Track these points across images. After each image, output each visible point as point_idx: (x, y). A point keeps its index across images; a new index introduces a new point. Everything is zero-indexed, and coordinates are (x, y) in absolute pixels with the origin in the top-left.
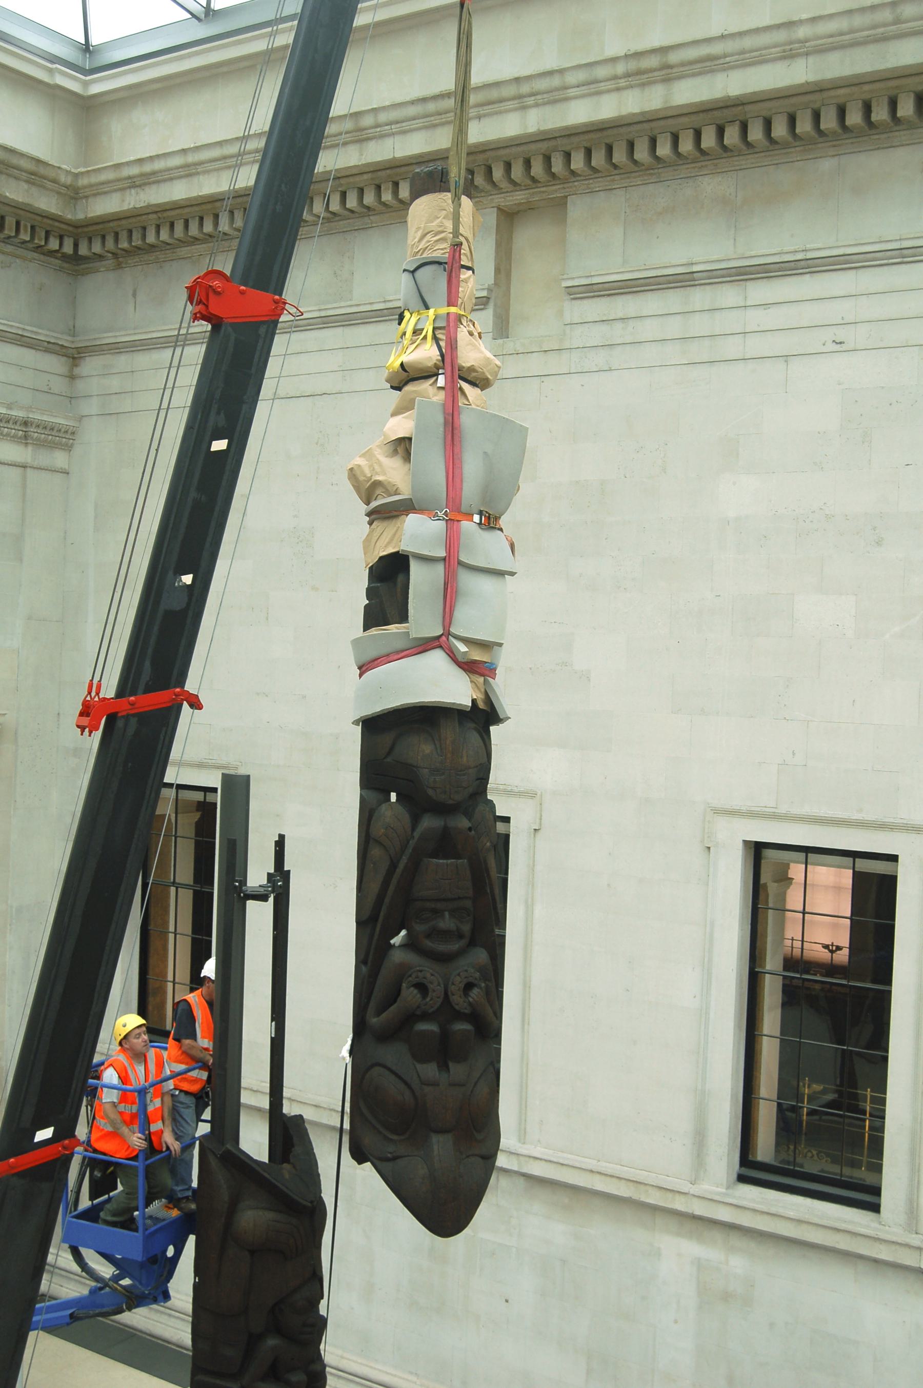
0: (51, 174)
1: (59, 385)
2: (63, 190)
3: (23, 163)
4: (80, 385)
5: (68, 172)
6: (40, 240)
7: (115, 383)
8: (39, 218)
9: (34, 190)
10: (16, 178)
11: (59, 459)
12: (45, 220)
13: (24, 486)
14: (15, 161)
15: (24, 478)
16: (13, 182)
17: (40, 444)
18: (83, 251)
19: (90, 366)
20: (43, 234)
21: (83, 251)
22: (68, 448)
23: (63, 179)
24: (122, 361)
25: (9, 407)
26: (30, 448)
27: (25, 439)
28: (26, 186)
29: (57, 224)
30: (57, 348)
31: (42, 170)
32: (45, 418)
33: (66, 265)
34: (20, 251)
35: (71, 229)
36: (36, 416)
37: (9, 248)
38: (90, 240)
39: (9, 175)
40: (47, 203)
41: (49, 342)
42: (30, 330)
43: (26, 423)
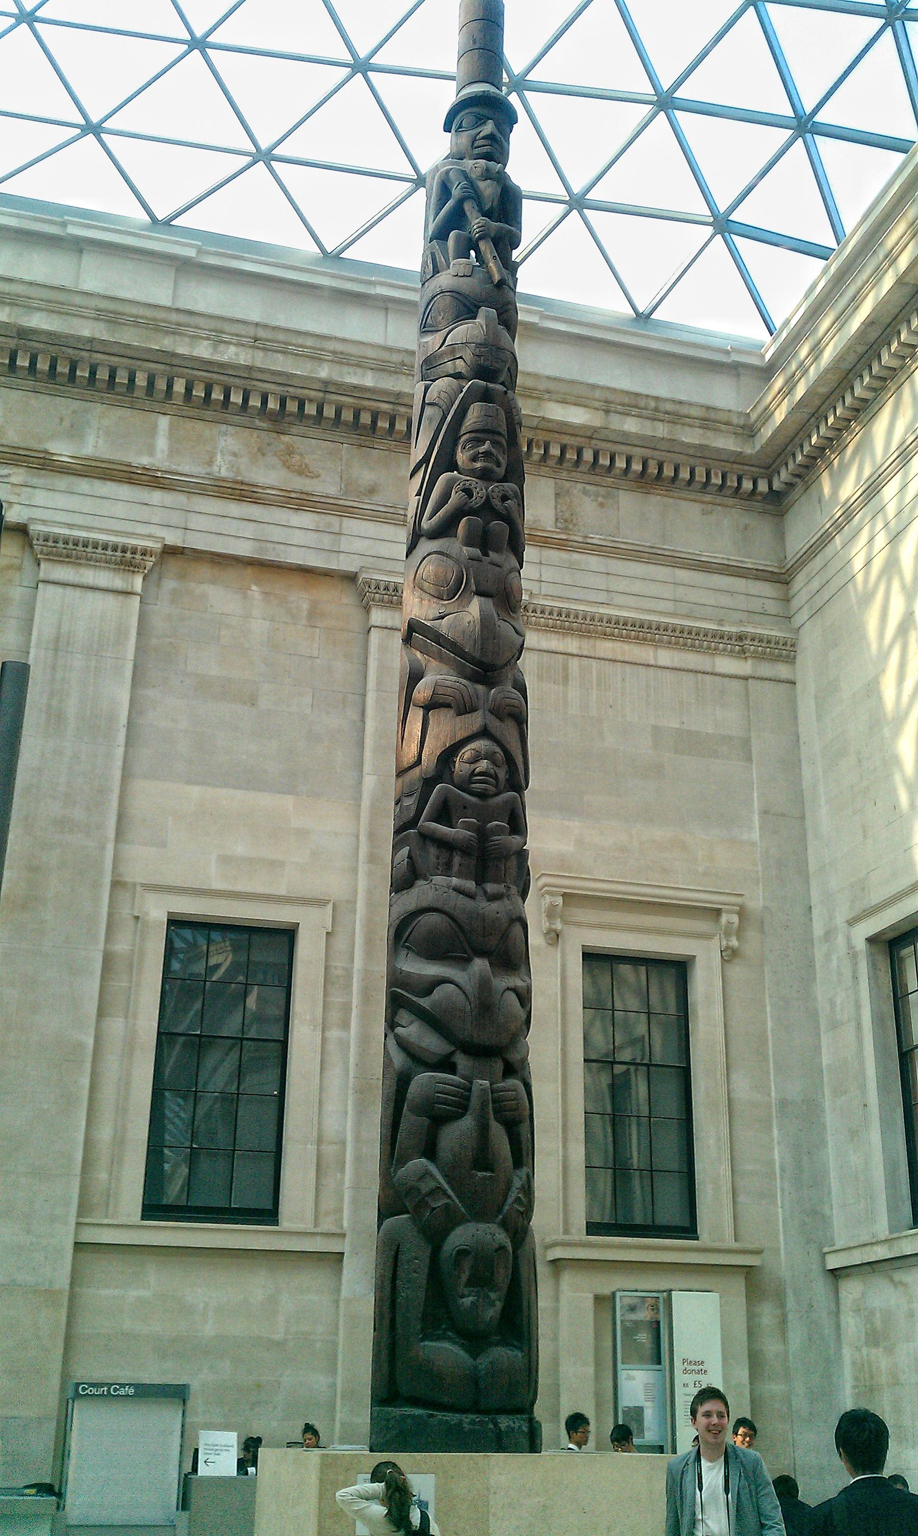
0: (722, 417)
1: (772, 607)
2: (740, 431)
3: (695, 412)
4: (795, 603)
5: (740, 414)
6: (732, 481)
7: (815, 584)
8: (728, 465)
9: (709, 434)
10: (690, 426)
11: (783, 670)
12: (735, 466)
13: (747, 695)
14: (685, 410)
15: (747, 689)
16: (687, 429)
17: (760, 657)
18: (776, 486)
19: (800, 580)
20: (735, 479)
21: (776, 486)
22: (791, 660)
23: (735, 420)
24: (818, 562)
25: (721, 622)
26: (750, 661)
27: (742, 654)
28: (700, 431)
29: (747, 468)
30: (769, 575)
31: (713, 415)
32: (759, 631)
33: (770, 507)
34: (719, 500)
35: (762, 471)
36: (750, 629)
37: (708, 498)
38: (779, 473)
39: (684, 424)
40: (726, 443)
41: (757, 570)
42: (734, 558)
43: (741, 638)
